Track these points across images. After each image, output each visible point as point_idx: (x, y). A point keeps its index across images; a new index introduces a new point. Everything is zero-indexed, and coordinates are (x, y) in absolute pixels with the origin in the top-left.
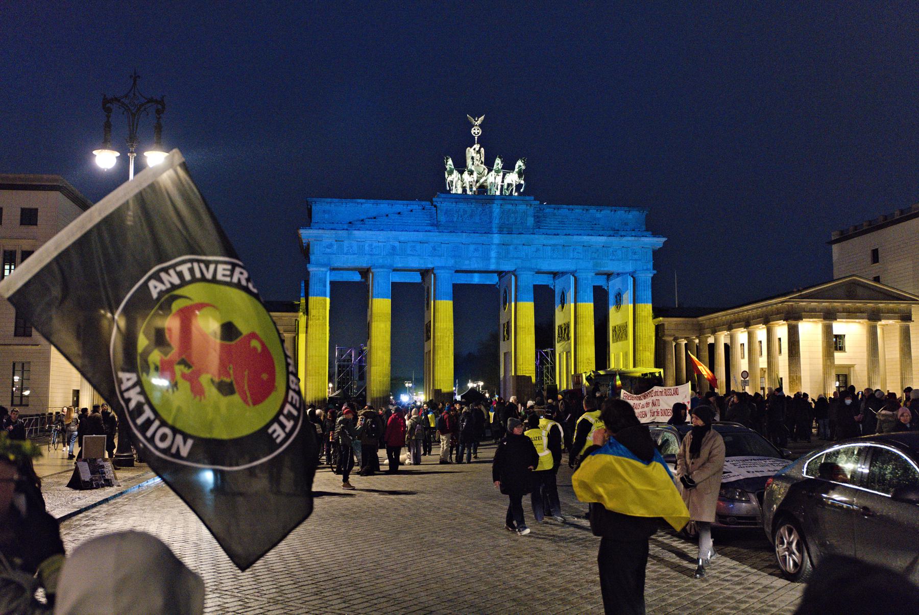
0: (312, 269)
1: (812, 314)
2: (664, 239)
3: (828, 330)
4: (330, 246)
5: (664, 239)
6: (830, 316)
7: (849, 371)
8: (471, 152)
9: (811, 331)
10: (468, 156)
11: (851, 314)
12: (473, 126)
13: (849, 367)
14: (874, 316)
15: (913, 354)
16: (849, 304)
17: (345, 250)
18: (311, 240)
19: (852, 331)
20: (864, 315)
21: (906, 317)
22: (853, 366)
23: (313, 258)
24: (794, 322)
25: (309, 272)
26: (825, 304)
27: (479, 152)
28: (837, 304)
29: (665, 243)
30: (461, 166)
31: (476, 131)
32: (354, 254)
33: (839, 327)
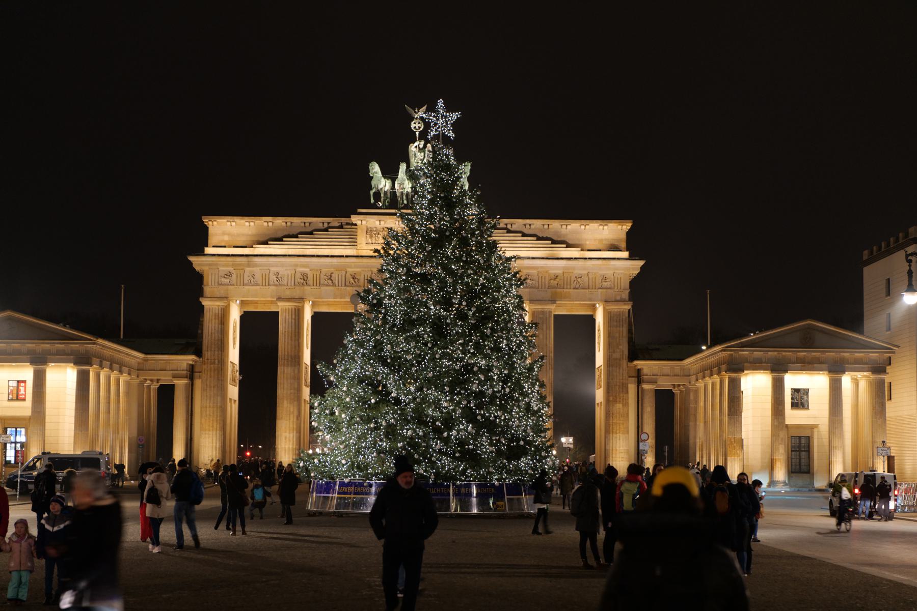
0: (205, 303)
1: (757, 365)
2: (641, 263)
3: (778, 386)
4: (229, 274)
5: (641, 263)
6: (778, 368)
7: (812, 433)
8: (413, 148)
9: (755, 385)
10: (411, 154)
11: (807, 366)
12: (413, 119)
13: (812, 427)
14: (836, 369)
15: (887, 415)
16: (802, 354)
17: (246, 282)
18: (205, 268)
19: (815, 383)
20: (824, 366)
21: (879, 369)
22: (816, 426)
23: (207, 290)
24: (734, 375)
25: (203, 307)
26: (772, 354)
27: (422, 150)
28: (788, 354)
29: (642, 268)
30: (390, 173)
31: (417, 126)
32: (258, 285)
33: (793, 380)
